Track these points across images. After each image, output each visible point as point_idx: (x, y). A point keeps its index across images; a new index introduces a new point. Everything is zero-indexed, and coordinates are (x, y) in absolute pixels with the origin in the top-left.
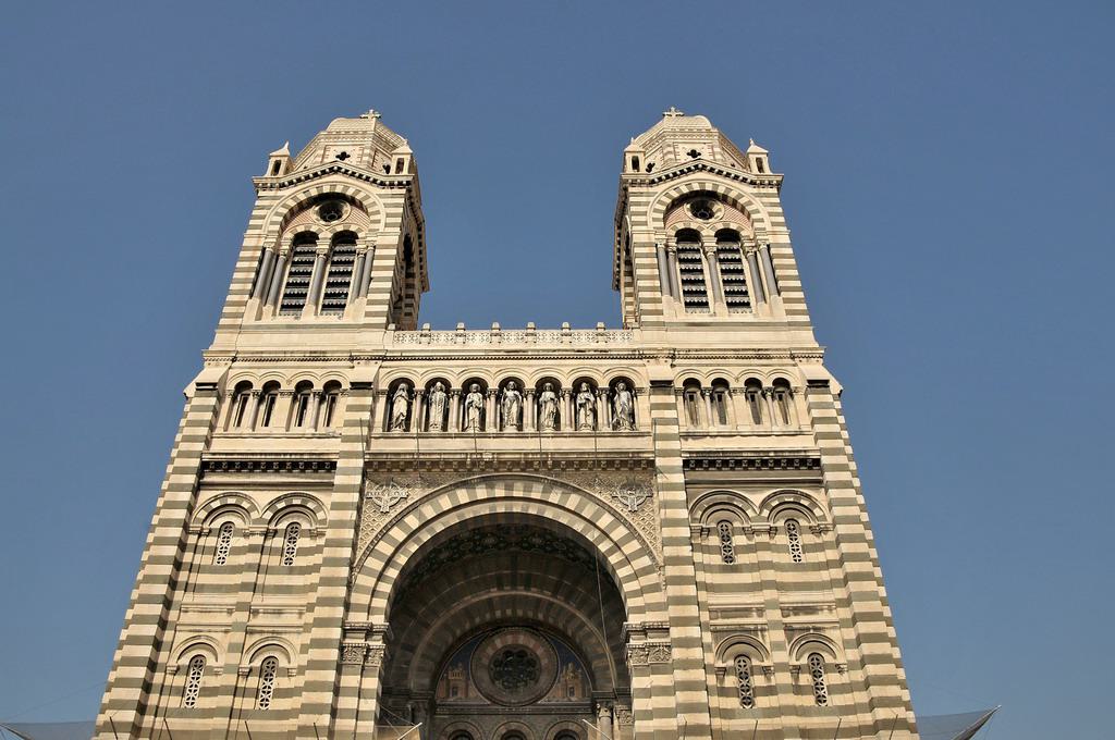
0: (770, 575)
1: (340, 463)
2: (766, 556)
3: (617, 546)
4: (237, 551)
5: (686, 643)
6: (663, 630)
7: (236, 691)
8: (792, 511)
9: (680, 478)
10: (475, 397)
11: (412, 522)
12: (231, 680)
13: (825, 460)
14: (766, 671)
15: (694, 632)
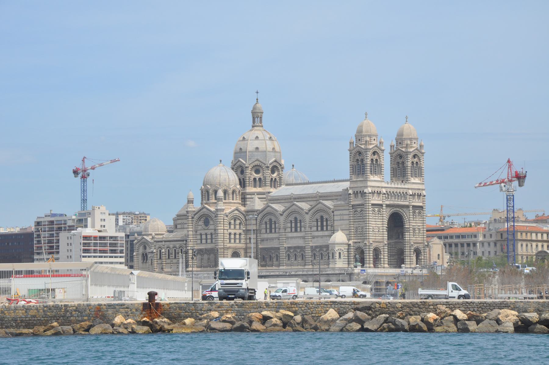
0: (417, 222)
1: (384, 205)
2: (417, 219)
3: (405, 217)
4: (374, 216)
5: (411, 230)
6: (409, 228)
7: (377, 234)
8: (420, 213)
9: (411, 209)
10: (393, 195)
11: (389, 213)
12: (376, 233)
13: (424, 207)
14: (416, 233)
15: (412, 229)
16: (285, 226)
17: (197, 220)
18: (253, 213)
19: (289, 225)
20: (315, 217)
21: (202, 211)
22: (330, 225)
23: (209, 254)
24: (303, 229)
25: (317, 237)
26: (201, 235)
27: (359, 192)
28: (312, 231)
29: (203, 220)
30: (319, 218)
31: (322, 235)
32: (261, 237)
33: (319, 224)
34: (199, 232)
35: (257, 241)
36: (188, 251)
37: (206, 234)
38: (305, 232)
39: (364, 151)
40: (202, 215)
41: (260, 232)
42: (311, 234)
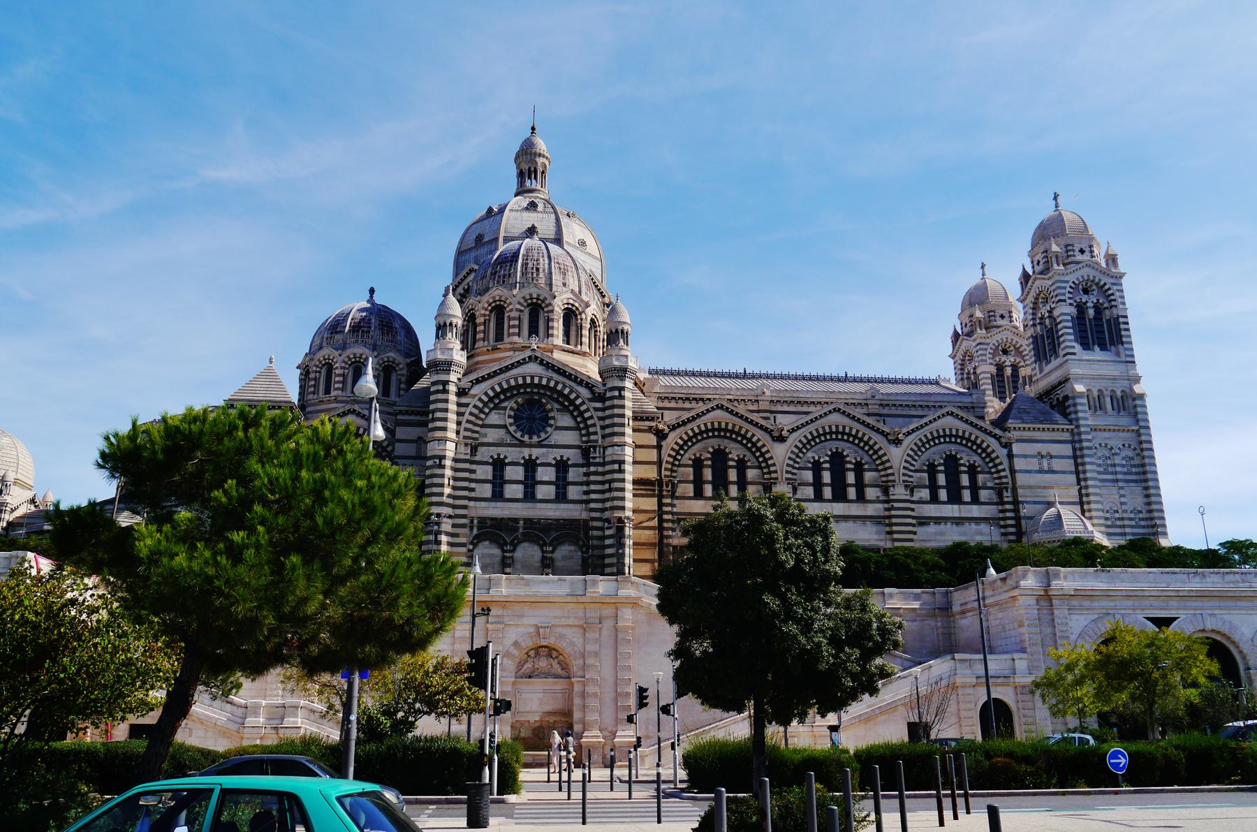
16: (795, 477)
17: (485, 404)
18: (647, 423)
19: (808, 476)
20: (923, 457)
21: (514, 372)
22: (989, 484)
23: (550, 545)
24: (871, 493)
25: (938, 520)
26: (499, 465)
27: (1107, 393)
28: (913, 502)
29: (512, 409)
30: (942, 461)
31: (957, 515)
32: (675, 510)
33: (941, 479)
34: (484, 454)
35: (661, 521)
36: (438, 524)
37: (530, 466)
38: (888, 502)
39: (1112, 281)
40: (518, 387)
41: (673, 491)
42: (913, 510)
